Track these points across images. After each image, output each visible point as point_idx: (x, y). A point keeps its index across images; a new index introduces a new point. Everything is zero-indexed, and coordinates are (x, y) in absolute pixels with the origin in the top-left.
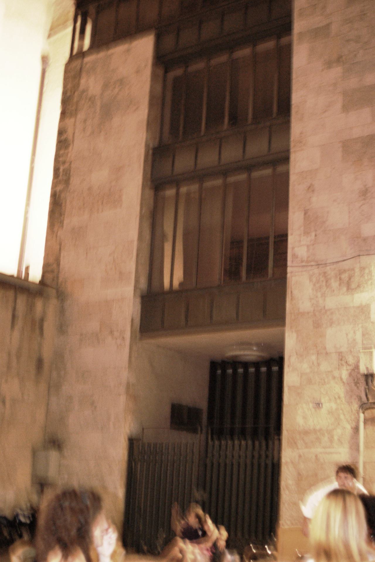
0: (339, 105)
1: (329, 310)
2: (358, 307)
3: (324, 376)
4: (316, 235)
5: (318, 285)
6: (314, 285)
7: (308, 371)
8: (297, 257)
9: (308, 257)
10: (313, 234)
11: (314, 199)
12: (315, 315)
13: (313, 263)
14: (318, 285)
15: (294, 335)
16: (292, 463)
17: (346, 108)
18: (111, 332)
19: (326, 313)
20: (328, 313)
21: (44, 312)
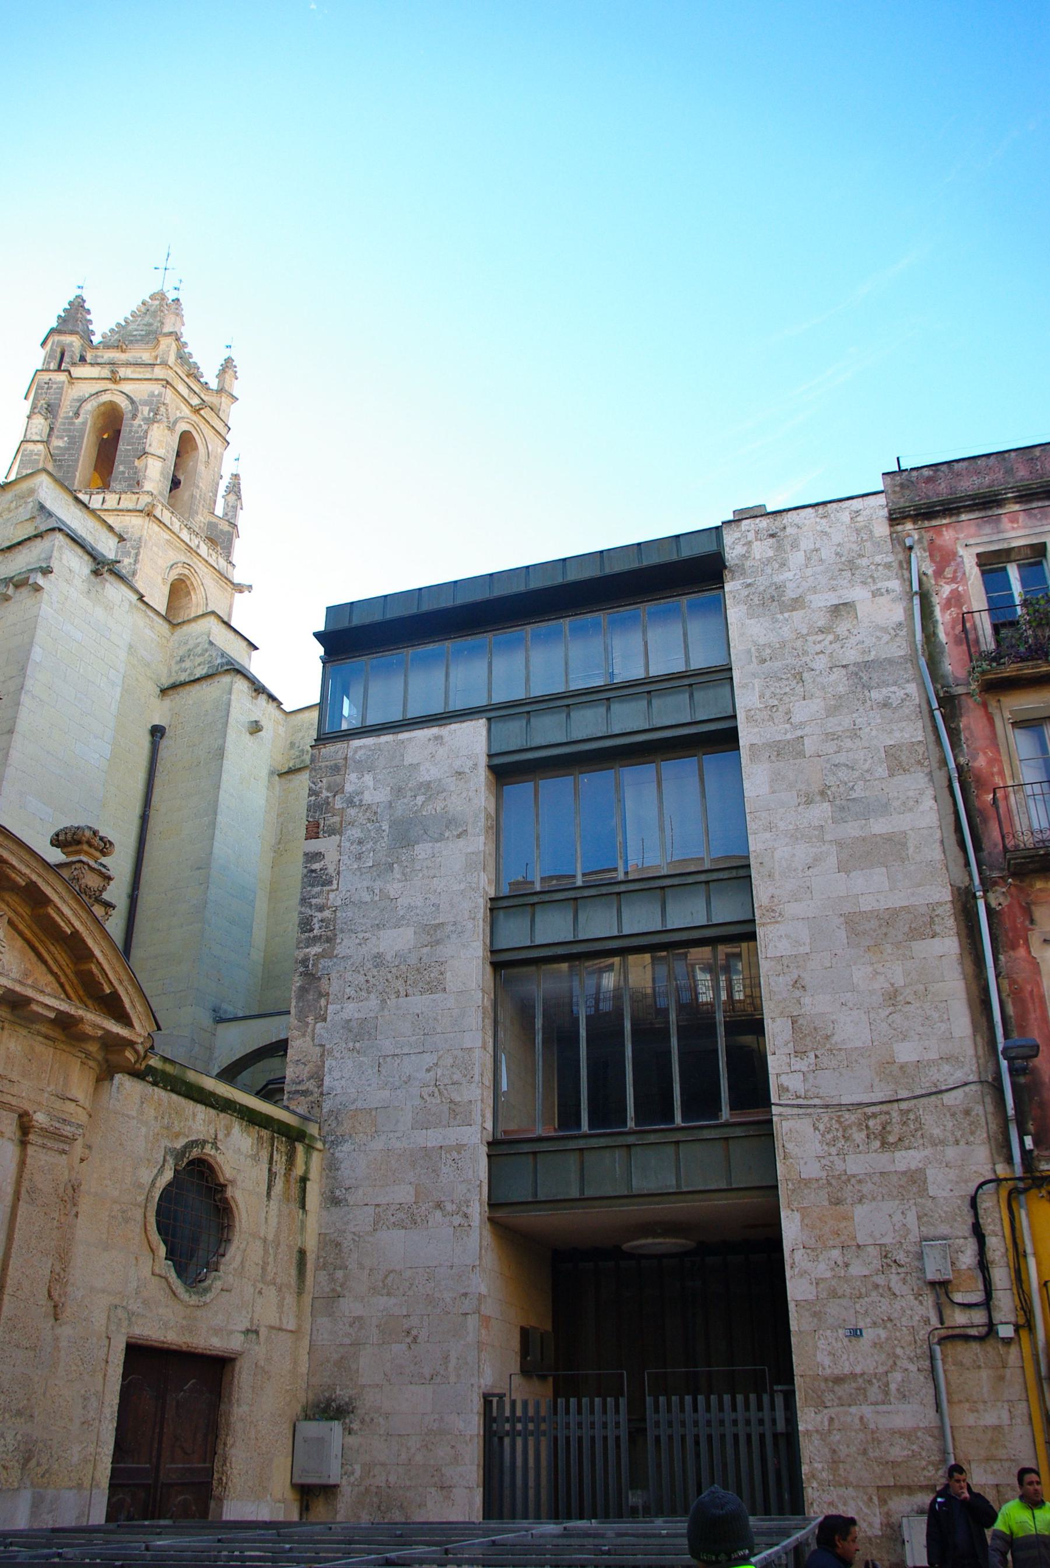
0: (832, 861)
1: (854, 1176)
2: (904, 1173)
3: (858, 1283)
4: (816, 1056)
5: (829, 1136)
6: (823, 1135)
7: (828, 1274)
8: (788, 1090)
9: (806, 1091)
10: (812, 1055)
11: (806, 1000)
12: (829, 1184)
13: (817, 1101)
14: (829, 1136)
15: (797, 1216)
16: (817, 1431)
17: (843, 868)
18: (439, 1205)
19: (849, 1180)
20: (853, 1181)
21: (307, 1171)
